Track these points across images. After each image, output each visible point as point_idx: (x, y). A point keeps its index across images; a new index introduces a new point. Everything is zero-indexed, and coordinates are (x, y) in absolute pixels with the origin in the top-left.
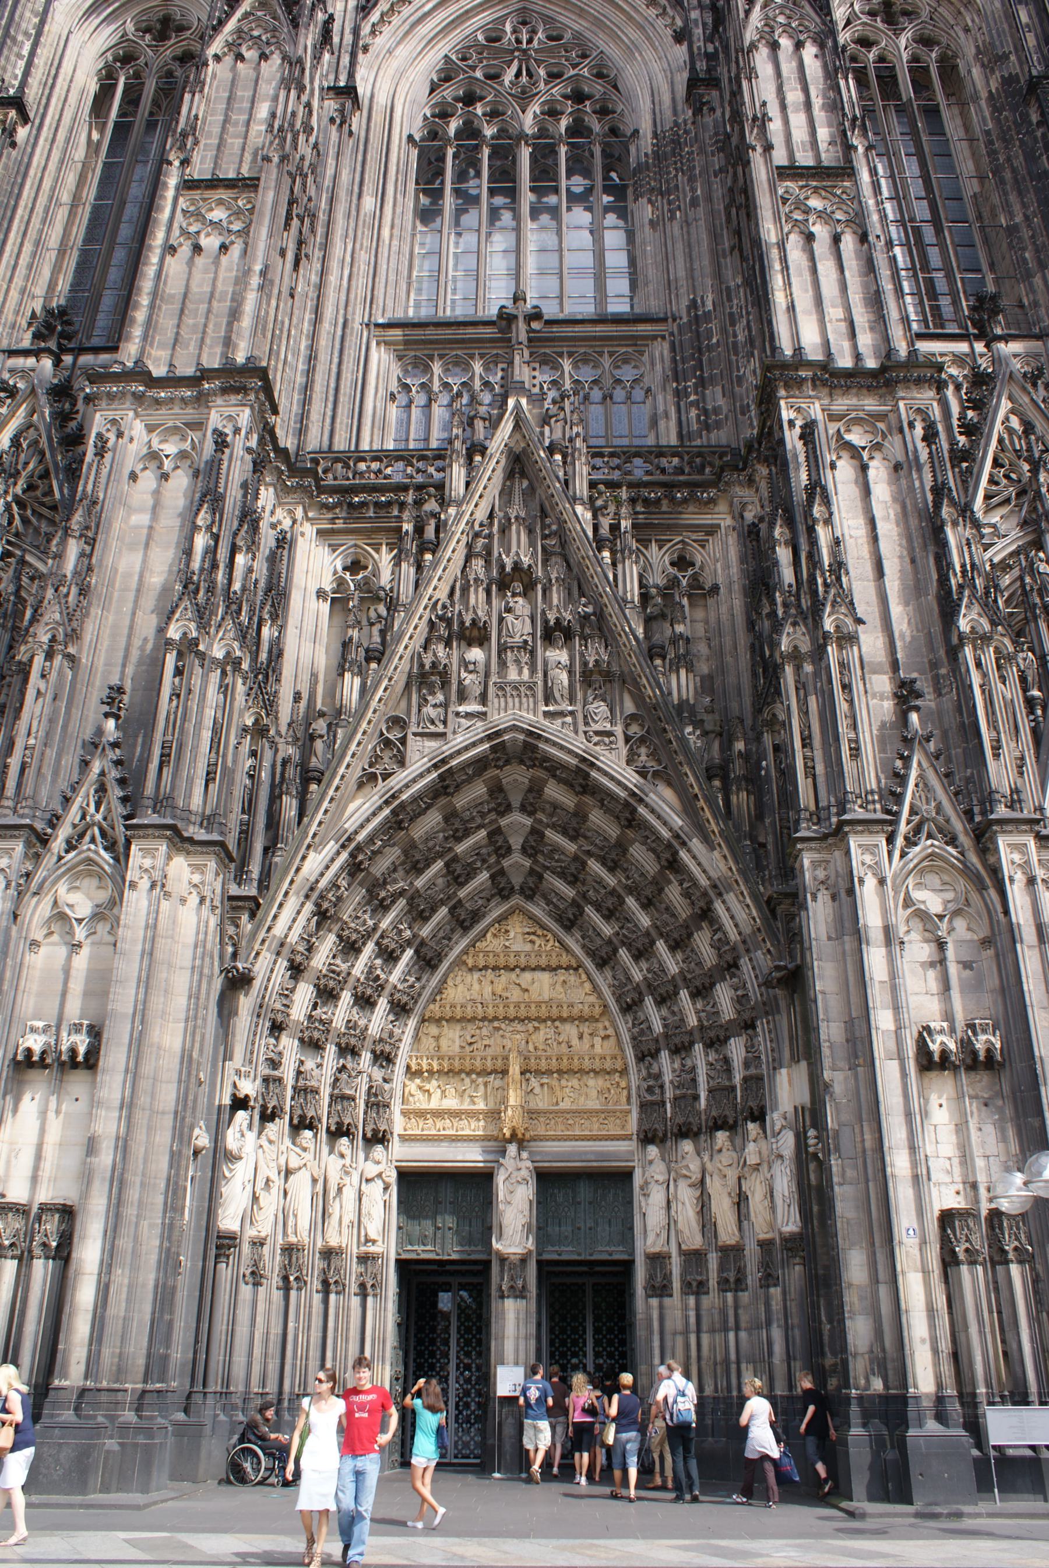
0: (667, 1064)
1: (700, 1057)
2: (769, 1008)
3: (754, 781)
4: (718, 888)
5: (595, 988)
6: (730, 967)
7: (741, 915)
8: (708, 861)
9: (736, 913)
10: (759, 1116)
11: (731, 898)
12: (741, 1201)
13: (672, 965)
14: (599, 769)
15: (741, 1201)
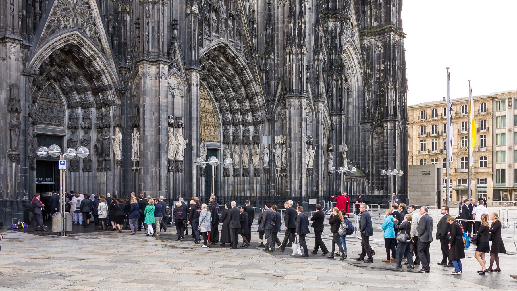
0: (231, 128)
1: (241, 129)
2: (262, 122)
3: (266, 72)
4: (257, 94)
5: (214, 107)
6: (253, 110)
7: (261, 101)
8: (255, 88)
9: (259, 101)
10: (258, 144)
11: (259, 97)
12: (251, 159)
13: (238, 106)
14: (239, 59)
15: (251, 159)
